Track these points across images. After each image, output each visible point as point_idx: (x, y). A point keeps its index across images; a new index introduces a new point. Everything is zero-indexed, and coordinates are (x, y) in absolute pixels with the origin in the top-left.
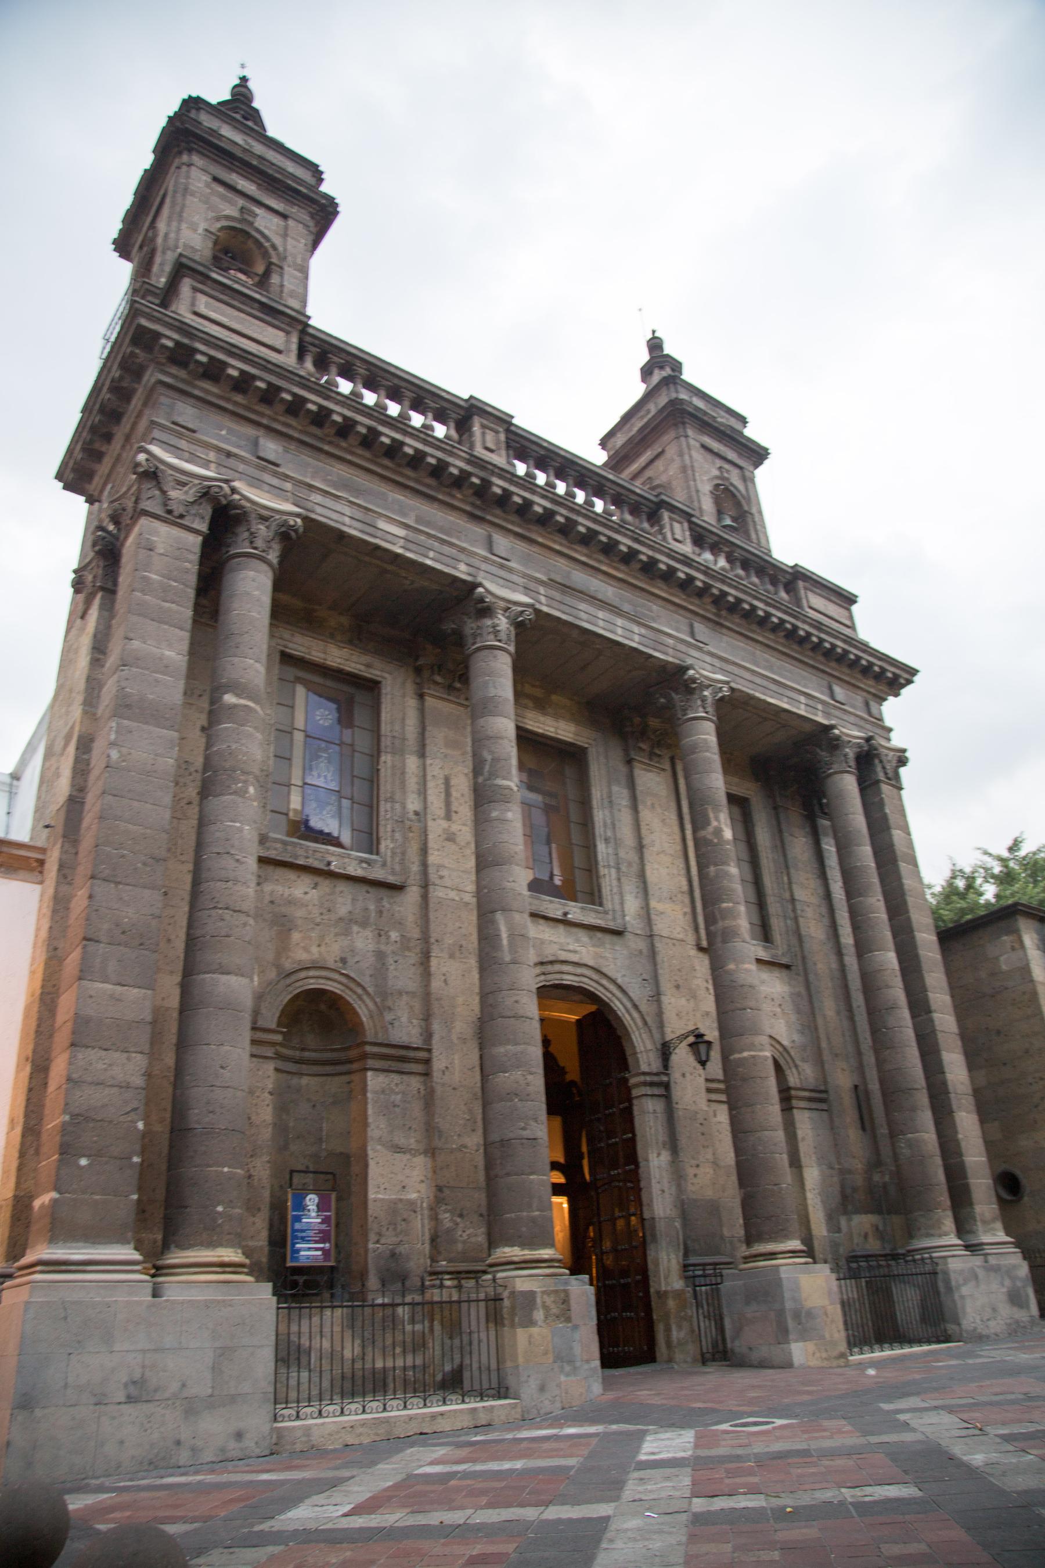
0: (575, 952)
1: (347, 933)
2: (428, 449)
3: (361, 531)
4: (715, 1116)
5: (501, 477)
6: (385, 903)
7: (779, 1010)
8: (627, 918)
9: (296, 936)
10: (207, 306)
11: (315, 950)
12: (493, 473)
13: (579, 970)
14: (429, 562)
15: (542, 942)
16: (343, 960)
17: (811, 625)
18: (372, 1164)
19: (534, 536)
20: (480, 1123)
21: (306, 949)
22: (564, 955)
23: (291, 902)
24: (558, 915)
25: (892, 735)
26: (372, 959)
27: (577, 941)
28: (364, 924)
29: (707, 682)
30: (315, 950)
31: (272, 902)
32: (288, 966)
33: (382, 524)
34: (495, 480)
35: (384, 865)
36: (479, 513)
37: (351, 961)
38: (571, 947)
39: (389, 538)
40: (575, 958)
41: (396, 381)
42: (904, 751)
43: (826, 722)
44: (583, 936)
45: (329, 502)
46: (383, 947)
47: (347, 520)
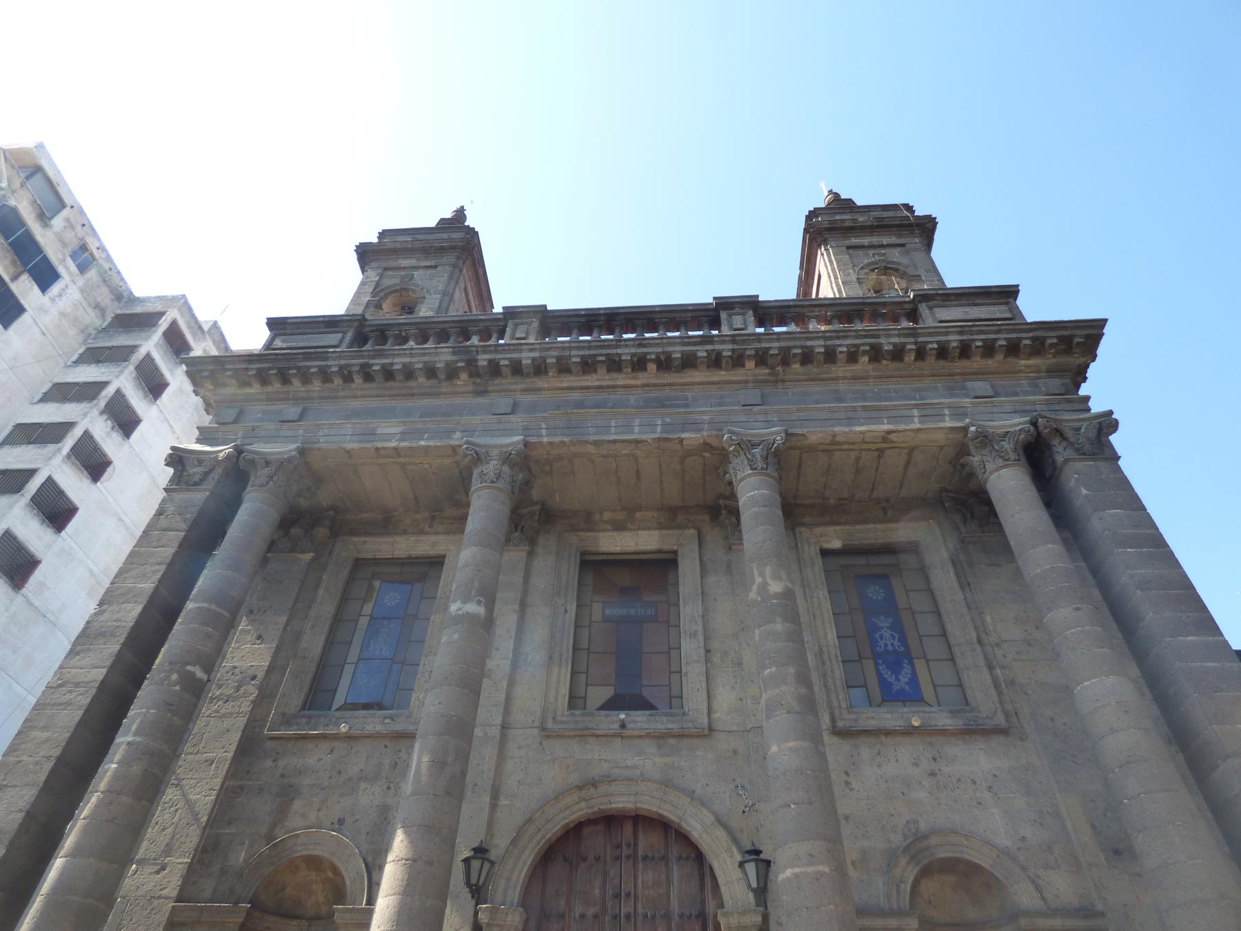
0: (635, 767)
2: (414, 360)
3: (361, 442)
5: (485, 352)
7: (987, 795)
8: (716, 715)
9: (297, 804)
10: (283, 341)
14: (422, 443)
16: (341, 822)
25: (1091, 404)
29: (757, 440)
31: (282, 776)
38: (629, 763)
41: (441, 326)
42: (1111, 413)
43: (960, 424)
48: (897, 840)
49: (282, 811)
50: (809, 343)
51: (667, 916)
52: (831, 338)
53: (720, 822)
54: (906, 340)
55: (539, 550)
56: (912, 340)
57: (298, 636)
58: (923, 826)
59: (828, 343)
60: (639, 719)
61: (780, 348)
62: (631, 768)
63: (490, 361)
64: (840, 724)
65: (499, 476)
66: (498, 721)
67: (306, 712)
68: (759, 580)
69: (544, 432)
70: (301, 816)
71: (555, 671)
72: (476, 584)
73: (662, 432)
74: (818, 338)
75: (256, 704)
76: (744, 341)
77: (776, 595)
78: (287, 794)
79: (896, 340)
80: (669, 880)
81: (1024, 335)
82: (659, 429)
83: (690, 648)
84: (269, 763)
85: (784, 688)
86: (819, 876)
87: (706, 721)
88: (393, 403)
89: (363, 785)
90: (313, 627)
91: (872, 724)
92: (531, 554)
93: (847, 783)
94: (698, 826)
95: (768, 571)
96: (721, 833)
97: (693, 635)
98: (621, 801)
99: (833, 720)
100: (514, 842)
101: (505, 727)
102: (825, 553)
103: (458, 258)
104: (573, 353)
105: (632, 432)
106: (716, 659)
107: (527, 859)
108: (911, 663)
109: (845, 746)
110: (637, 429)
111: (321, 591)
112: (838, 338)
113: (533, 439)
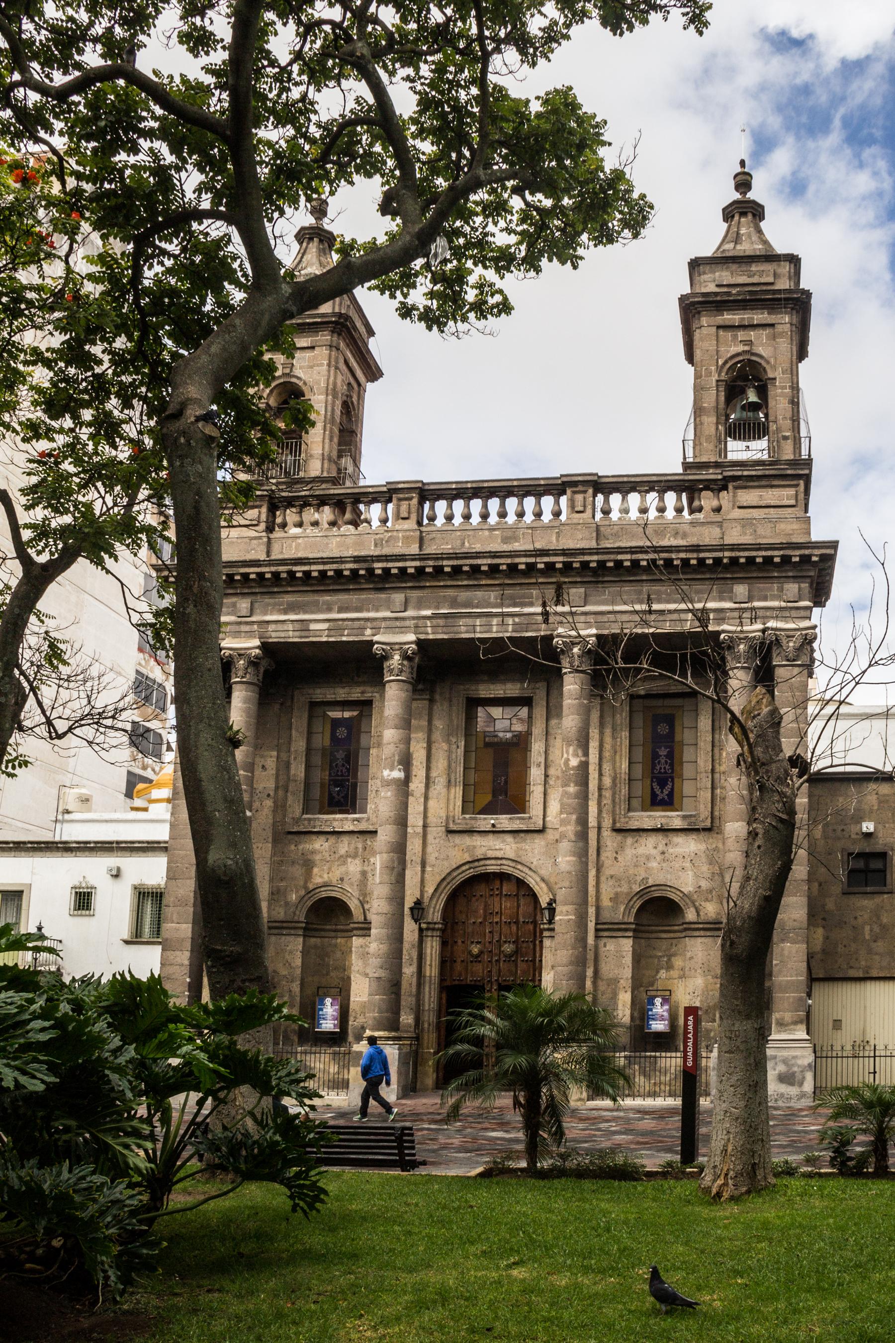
1: (344, 863)
3: (301, 637)
4: (605, 946)
6: (369, 843)
8: (548, 819)
9: (315, 870)
11: (326, 876)
12: (373, 561)
13: (499, 862)
14: (344, 639)
15: (475, 847)
16: (342, 879)
17: (686, 551)
18: (353, 984)
19: (422, 584)
20: (415, 961)
21: (321, 876)
22: (490, 854)
23: (313, 852)
24: (488, 828)
26: (358, 876)
27: (504, 841)
28: (355, 857)
30: (326, 876)
32: (311, 887)
33: (313, 626)
34: (376, 565)
35: (368, 819)
36: (380, 586)
37: (346, 879)
39: (318, 633)
40: (499, 854)
44: (509, 838)
45: (280, 627)
46: (366, 868)
47: (291, 633)
48: (636, 888)
49: (308, 875)
50: (620, 557)
51: (517, 923)
52: (636, 553)
53: (543, 880)
54: (689, 555)
55: (437, 697)
56: (695, 555)
57: (288, 765)
58: (651, 882)
59: (635, 557)
60: (504, 821)
61: (598, 562)
62: (499, 850)
63: (383, 569)
64: (618, 825)
65: (401, 671)
66: (421, 823)
67: (305, 816)
68: (565, 756)
69: (429, 630)
70: (320, 876)
71: (453, 791)
72: (397, 758)
73: (513, 631)
74: (627, 553)
75: (275, 811)
76: (572, 554)
77: (573, 768)
78: (308, 865)
79: (683, 555)
80: (518, 906)
81: (776, 553)
82: (510, 628)
83: (535, 774)
84: (293, 847)
85: (569, 827)
86: (569, 921)
87: (541, 823)
88: (316, 597)
89: (349, 860)
90: (295, 758)
91: (635, 825)
92: (432, 701)
93: (616, 858)
94: (532, 881)
95: (571, 749)
96: (543, 885)
97: (539, 765)
98: (491, 869)
99: (614, 822)
100: (436, 890)
101: (425, 826)
102: (632, 697)
103: (333, 332)
104: (445, 563)
105: (490, 631)
106: (551, 782)
107: (443, 897)
108: (673, 781)
109: (619, 837)
110: (495, 629)
111: (294, 732)
112: (641, 552)
113: (422, 637)
